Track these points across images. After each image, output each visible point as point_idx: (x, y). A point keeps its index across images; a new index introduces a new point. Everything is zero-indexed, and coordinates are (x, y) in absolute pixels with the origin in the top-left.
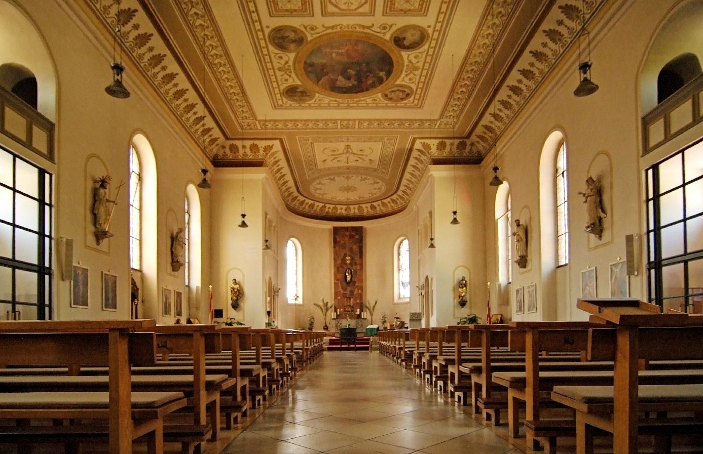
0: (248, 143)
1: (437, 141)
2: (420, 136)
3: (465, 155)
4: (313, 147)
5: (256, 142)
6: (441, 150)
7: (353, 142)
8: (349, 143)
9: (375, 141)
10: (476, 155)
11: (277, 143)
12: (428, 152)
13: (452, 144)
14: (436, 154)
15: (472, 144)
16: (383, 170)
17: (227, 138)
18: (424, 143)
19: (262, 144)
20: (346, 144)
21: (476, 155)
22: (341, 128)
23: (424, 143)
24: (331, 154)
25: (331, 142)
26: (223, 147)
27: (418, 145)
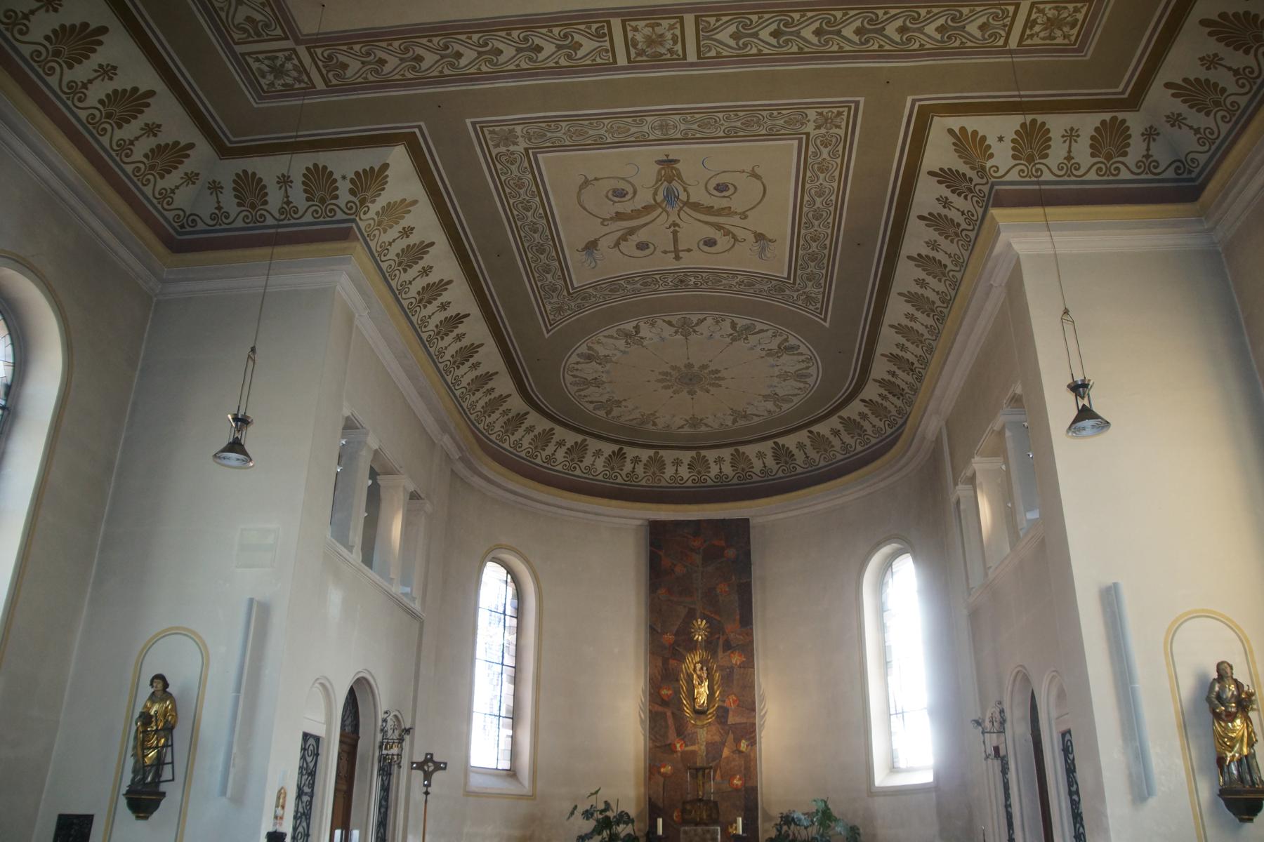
0: (299, 164)
1: (1010, 124)
2: (951, 97)
3: (1125, 175)
4: (534, 169)
5: (326, 159)
6: (1030, 159)
7: (685, 139)
8: (673, 150)
9: (772, 135)
10: (1170, 174)
11: (398, 157)
12: (982, 171)
13: (1071, 135)
14: (1013, 176)
15: (1150, 134)
16: (810, 288)
17: (224, 152)
18: (963, 129)
19: (344, 164)
20: (660, 151)
21: (1170, 174)
22: (632, 65)
23: (963, 129)
24: (609, 209)
25: (600, 144)
26: (215, 187)
27: (939, 153)
